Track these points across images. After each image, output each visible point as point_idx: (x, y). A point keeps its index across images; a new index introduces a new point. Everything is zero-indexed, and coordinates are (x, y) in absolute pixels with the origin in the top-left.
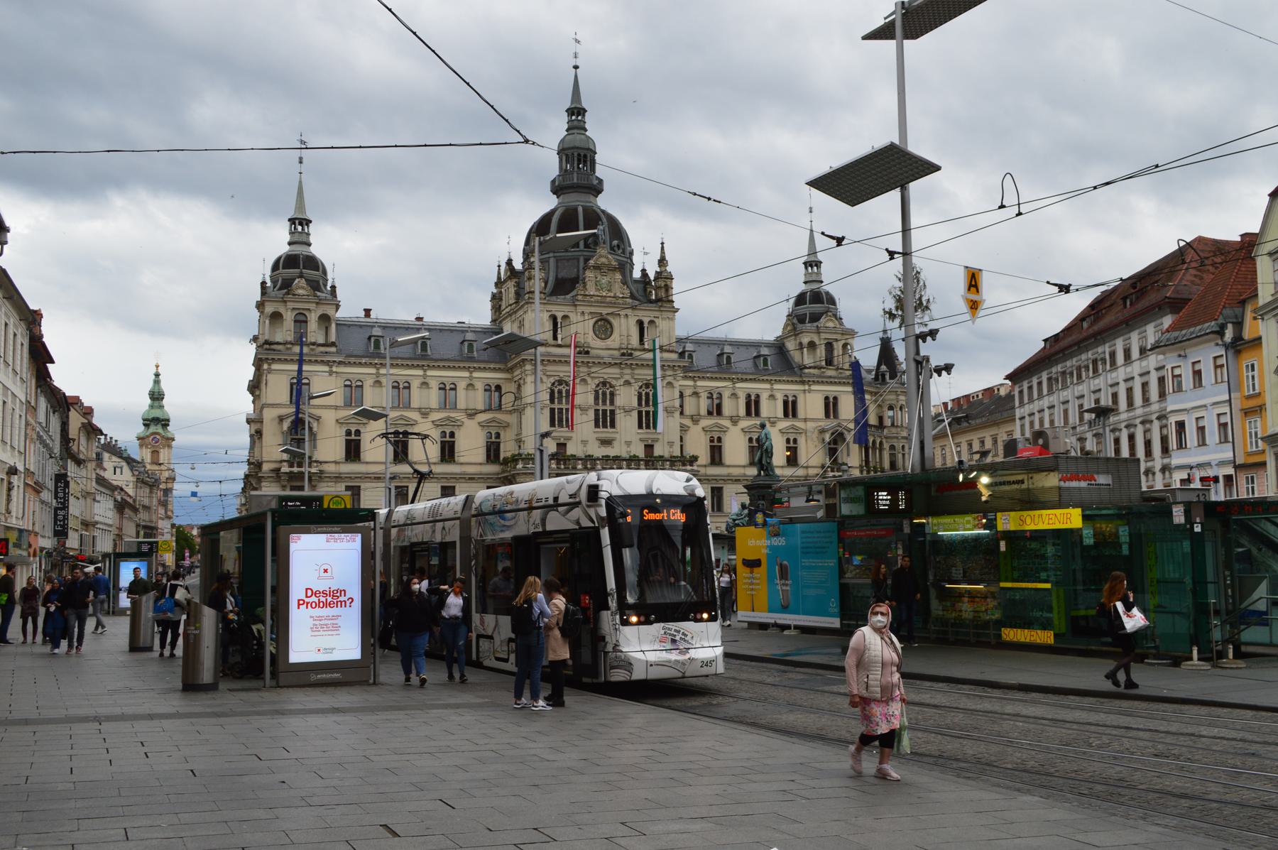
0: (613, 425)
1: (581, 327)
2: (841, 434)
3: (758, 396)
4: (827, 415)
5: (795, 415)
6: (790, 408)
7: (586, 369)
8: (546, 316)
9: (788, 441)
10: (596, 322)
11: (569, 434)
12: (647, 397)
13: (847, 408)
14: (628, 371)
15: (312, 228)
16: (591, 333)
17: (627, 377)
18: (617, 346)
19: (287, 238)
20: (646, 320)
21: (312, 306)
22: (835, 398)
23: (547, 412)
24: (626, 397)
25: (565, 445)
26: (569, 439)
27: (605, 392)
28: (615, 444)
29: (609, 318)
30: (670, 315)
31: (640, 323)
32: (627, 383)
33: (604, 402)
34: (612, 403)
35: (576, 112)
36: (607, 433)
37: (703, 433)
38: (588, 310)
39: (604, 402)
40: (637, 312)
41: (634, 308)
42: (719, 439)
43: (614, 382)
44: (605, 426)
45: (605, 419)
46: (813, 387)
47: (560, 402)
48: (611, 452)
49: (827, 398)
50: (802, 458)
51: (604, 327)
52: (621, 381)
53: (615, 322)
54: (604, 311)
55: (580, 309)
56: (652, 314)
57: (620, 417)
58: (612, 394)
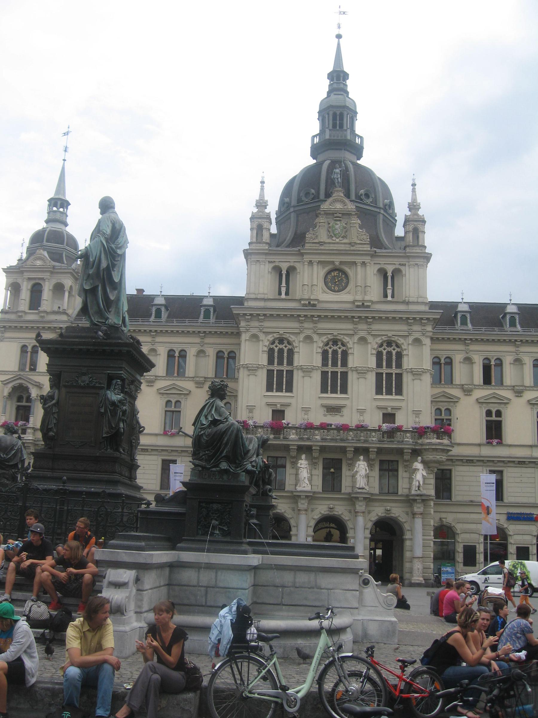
0: (344, 390)
1: (310, 281)
7: (311, 325)
8: (268, 267)
10: (329, 273)
15: (71, 211)
16: (321, 284)
19: (45, 217)
20: (390, 269)
21: (46, 275)
24: (362, 357)
25: (283, 412)
26: (288, 405)
28: (345, 411)
29: (347, 269)
30: (420, 261)
31: (383, 273)
35: (338, 78)
36: (334, 399)
37: (477, 407)
38: (316, 258)
40: (377, 260)
41: (374, 255)
42: (499, 413)
47: (280, 363)
48: (335, 420)
51: (337, 278)
53: (350, 272)
54: (337, 260)
55: (307, 258)
56: (397, 261)
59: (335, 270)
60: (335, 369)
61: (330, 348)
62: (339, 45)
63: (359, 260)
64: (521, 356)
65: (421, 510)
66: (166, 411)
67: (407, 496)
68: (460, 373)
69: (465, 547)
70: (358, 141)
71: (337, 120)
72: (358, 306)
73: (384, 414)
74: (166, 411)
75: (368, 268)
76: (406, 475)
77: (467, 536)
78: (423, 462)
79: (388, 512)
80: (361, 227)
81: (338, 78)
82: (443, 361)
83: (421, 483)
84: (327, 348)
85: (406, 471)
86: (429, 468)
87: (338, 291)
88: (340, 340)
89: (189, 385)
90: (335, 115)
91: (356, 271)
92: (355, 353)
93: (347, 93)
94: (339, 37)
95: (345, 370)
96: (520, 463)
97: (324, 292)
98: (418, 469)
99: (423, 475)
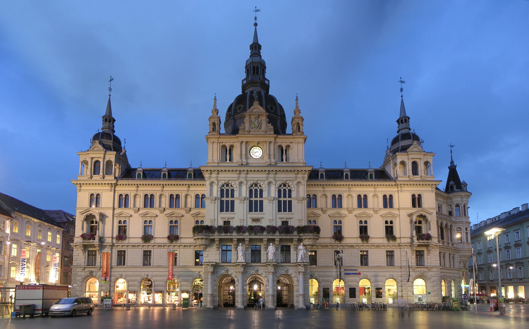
2: (424, 217)
3: (365, 196)
4: (414, 205)
5: (391, 206)
6: (388, 202)
9: (386, 222)
13: (429, 201)
22: (420, 196)
35: (256, 47)
42: (340, 222)
46: (404, 189)
49: (413, 196)
50: (396, 233)
62: (256, 29)
64: (351, 193)
66: (170, 226)
68: (321, 202)
69: (323, 288)
70: (266, 82)
71: (256, 69)
74: (170, 226)
77: (325, 283)
81: (256, 47)
82: (311, 197)
90: (254, 67)
93: (261, 56)
94: (256, 25)
96: (351, 246)
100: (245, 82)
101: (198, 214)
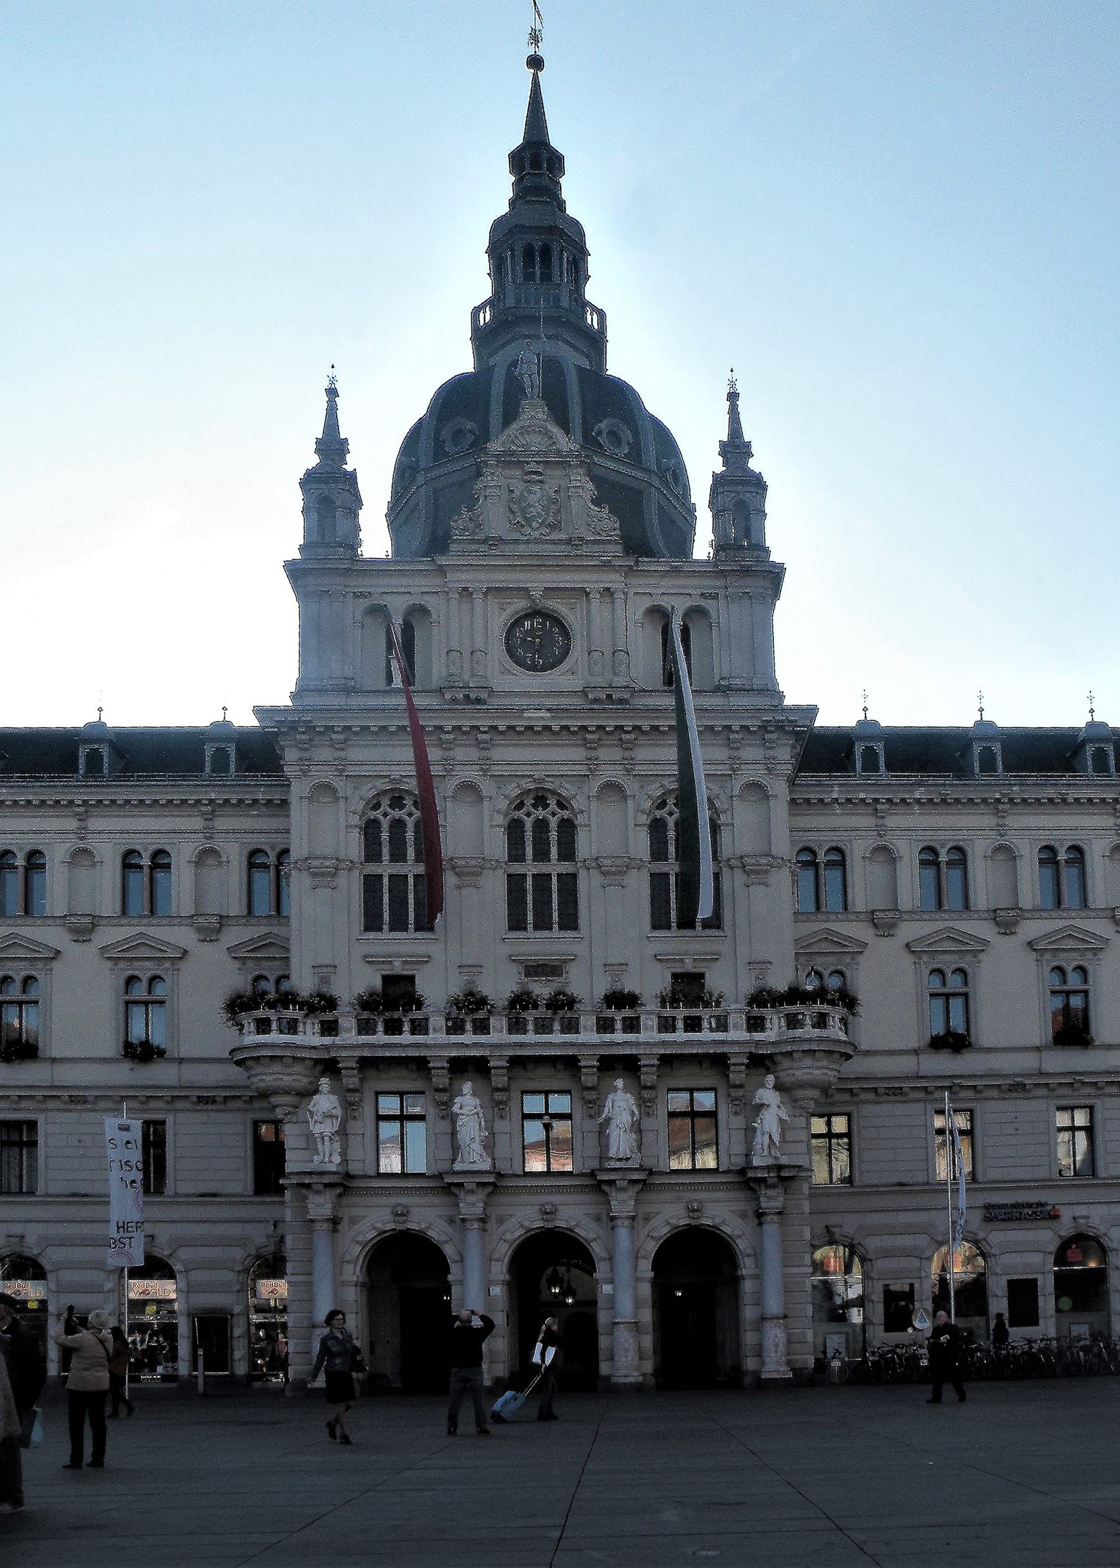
0: (570, 922)
10: (518, 622)
11: (422, 949)
12: (679, 833)
14: (610, 753)
16: (498, 650)
17: (610, 773)
18: (577, 683)
23: (352, 887)
24: (614, 831)
27: (541, 829)
31: (660, 615)
32: (613, 788)
33: (542, 855)
34: (568, 852)
39: (542, 855)
43: (567, 790)
44: (542, 923)
45: (544, 905)
52: (595, 785)
53: (573, 618)
57: (588, 885)
58: (568, 828)
59: (534, 613)
60: (543, 868)
61: (528, 815)
63: (592, 581)
65: (778, 1203)
67: (742, 1172)
72: (596, 701)
73: (675, 976)
75: (619, 603)
76: (738, 1122)
78: (777, 1087)
79: (696, 1214)
80: (596, 502)
83: (777, 1139)
84: (521, 814)
85: (736, 1113)
86: (795, 1101)
87: (543, 669)
88: (554, 792)
89: (183, 936)
91: (589, 613)
92: (593, 822)
95: (571, 870)
97: (505, 671)
98: (768, 1106)
99: (781, 1120)
100: (486, 317)
101: (261, 945)
